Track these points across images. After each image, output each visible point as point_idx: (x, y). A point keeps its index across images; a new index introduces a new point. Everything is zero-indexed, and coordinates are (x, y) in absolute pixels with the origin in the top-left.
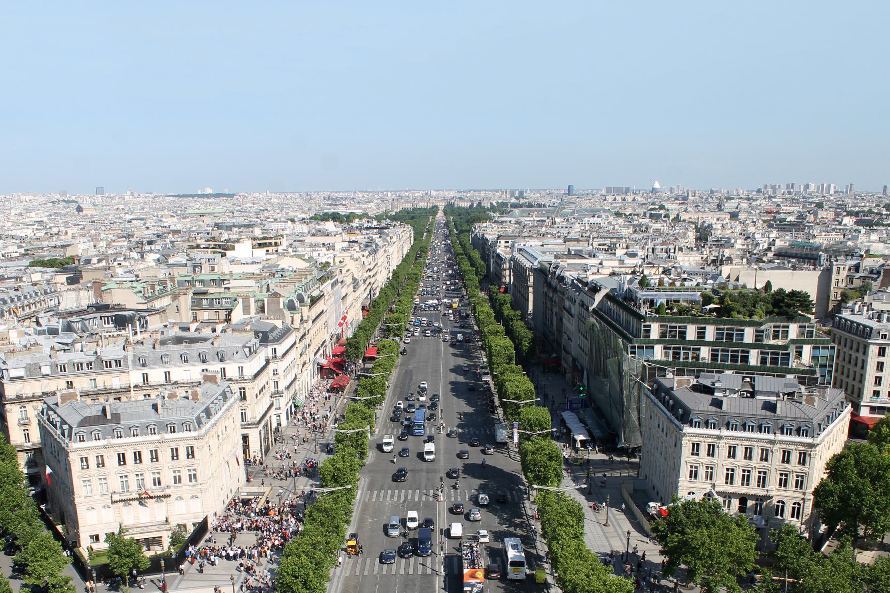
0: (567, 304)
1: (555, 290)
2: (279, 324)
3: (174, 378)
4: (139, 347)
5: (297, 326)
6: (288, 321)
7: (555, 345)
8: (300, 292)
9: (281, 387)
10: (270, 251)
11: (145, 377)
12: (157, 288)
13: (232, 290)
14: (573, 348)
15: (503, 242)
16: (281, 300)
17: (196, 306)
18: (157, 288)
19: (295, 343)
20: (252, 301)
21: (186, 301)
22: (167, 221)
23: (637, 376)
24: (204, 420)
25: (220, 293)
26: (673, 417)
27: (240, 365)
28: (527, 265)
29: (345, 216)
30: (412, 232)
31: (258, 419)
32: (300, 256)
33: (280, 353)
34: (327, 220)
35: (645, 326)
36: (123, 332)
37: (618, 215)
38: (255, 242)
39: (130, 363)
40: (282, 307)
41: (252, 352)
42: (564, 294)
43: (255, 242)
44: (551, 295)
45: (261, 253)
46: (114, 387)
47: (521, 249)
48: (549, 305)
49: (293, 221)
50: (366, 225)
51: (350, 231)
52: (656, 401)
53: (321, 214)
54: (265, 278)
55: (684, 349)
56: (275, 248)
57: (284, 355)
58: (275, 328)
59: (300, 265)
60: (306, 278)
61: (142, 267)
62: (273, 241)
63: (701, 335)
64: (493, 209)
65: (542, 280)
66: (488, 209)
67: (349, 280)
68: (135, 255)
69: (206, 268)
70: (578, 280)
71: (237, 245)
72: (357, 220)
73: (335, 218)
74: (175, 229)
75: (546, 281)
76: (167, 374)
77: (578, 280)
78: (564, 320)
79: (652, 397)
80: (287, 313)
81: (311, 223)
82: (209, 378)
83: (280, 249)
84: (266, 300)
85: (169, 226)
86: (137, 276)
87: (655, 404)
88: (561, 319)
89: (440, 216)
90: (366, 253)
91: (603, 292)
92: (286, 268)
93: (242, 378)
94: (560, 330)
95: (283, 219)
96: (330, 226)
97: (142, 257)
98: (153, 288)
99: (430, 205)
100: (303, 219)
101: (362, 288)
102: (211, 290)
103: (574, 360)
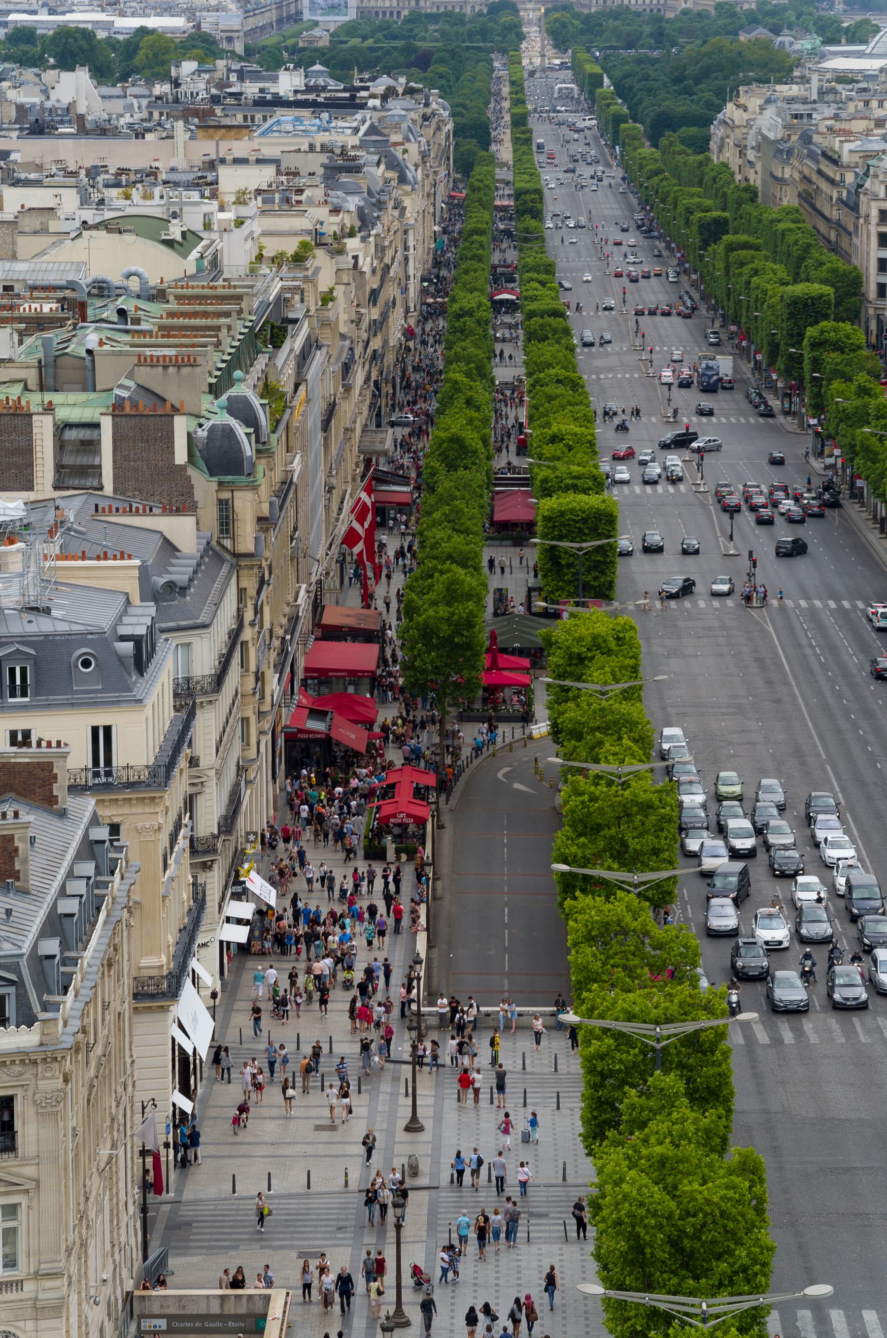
6: (210, 513)
16: (181, 426)
24: (55, 971)
27: (101, 719)
29: (112, 44)
40: (181, 456)
50: (251, 89)
51: (202, 118)
54: (39, 323)
57: (219, 679)
72: (189, 67)
80: (204, 487)
92: (115, 279)
96: (74, 87)
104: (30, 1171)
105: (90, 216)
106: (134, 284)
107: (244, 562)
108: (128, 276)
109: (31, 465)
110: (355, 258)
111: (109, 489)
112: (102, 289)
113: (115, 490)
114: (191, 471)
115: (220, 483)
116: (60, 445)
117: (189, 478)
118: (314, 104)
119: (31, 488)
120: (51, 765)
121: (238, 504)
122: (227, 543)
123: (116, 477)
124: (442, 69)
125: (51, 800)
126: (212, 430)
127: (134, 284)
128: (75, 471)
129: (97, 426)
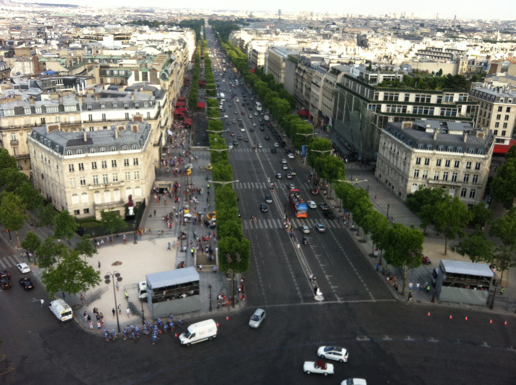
0: (314, 80)
1: (304, 72)
2: (159, 87)
3: (108, 118)
4: (85, 98)
5: (167, 89)
6: (162, 85)
7: (304, 104)
11: (90, 116)
12: (73, 62)
13: (124, 66)
14: (320, 106)
16: (158, 73)
17: (103, 74)
18: (73, 62)
20: (140, 73)
21: (95, 72)
22: (43, 20)
23: (372, 121)
24: (142, 143)
25: (116, 67)
26: (404, 144)
28: (281, 57)
31: (157, 140)
32: (155, 47)
33: (162, 104)
34: (141, 24)
35: (376, 94)
36: (71, 89)
37: (311, 28)
39: (81, 108)
40: (158, 77)
41: (154, 104)
42: (311, 74)
44: (301, 74)
45: (119, 43)
46: (71, 122)
48: (299, 80)
49: (122, 25)
50: (169, 29)
52: (390, 135)
53: (136, 21)
54: (140, 59)
55: (398, 106)
56: (127, 41)
57: (164, 106)
58: (157, 89)
59: (156, 52)
61: (50, 48)
63: (407, 99)
64: (236, 22)
65: (294, 65)
66: (234, 22)
67: (179, 63)
68: (41, 40)
69: (94, 51)
70: (321, 66)
71: (104, 38)
72: (161, 26)
73: (146, 23)
74: (47, 25)
75: (296, 67)
76: (104, 115)
77: (321, 66)
78: (312, 90)
79: (386, 132)
80: (162, 81)
81: (133, 26)
82: (138, 119)
83: (130, 41)
84: (149, 73)
85: (43, 23)
86: (58, 54)
87: (386, 136)
88: (310, 89)
89: (207, 25)
90: (182, 46)
91: (343, 74)
92: (150, 53)
93: (149, 119)
94: (308, 95)
95: (113, 23)
96: (146, 28)
97: (46, 42)
98: (71, 62)
99: (199, 18)
100: (126, 24)
102: (111, 65)
103: (320, 113)
104: (140, 167)
105: (147, 45)
111: (149, 81)
112: (148, 55)
116: (143, 76)
120: (16, 114)
125: (141, 121)
127: (152, 54)
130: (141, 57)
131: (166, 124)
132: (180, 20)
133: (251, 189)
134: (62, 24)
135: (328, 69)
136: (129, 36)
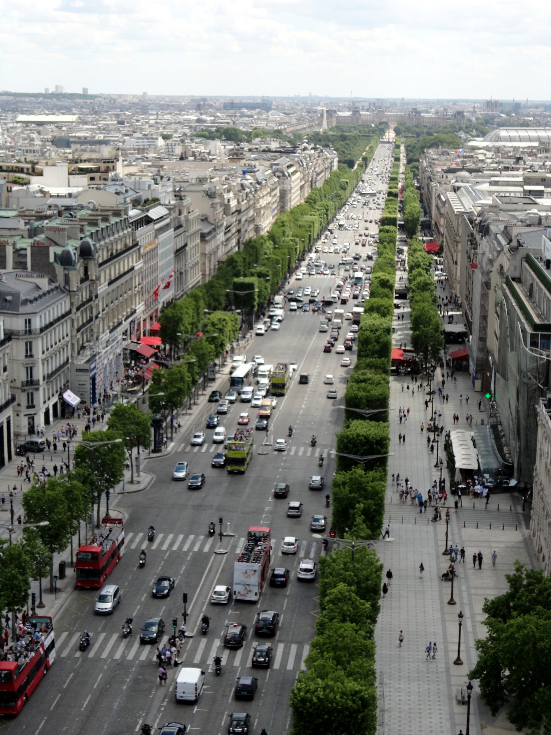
8: (89, 240)
9: (39, 373)
10: (97, 178)
15: (450, 176)
16: (53, 250)
19: (70, 312)
30: (336, 160)
33: (37, 324)
38: (74, 166)
40: (52, 259)
43: (74, 166)
47: (459, 188)
53: (213, 129)
56: (104, 175)
58: (38, 288)
60: (105, 219)
62: (103, 166)
73: (230, 135)
80: (59, 269)
92: (85, 204)
101: (221, 237)
106: (91, 206)
107: (72, 293)
108: (89, 203)
109: (5, 261)
110: (229, 201)
111: (29, 269)
113: (32, 270)
114: (55, 264)
115: (64, 269)
117: (54, 267)
118: (281, 152)
119: (5, 268)
121: (70, 275)
122: (67, 287)
123: (32, 266)
124: (347, 142)
126: (63, 252)
127: (91, 206)
128: (20, 264)
129: (25, 249)
130: (49, 213)
131: (49, 377)
132: (324, 128)
133: (166, 551)
134: (32, 140)
135: (511, 241)
136: (111, 165)
